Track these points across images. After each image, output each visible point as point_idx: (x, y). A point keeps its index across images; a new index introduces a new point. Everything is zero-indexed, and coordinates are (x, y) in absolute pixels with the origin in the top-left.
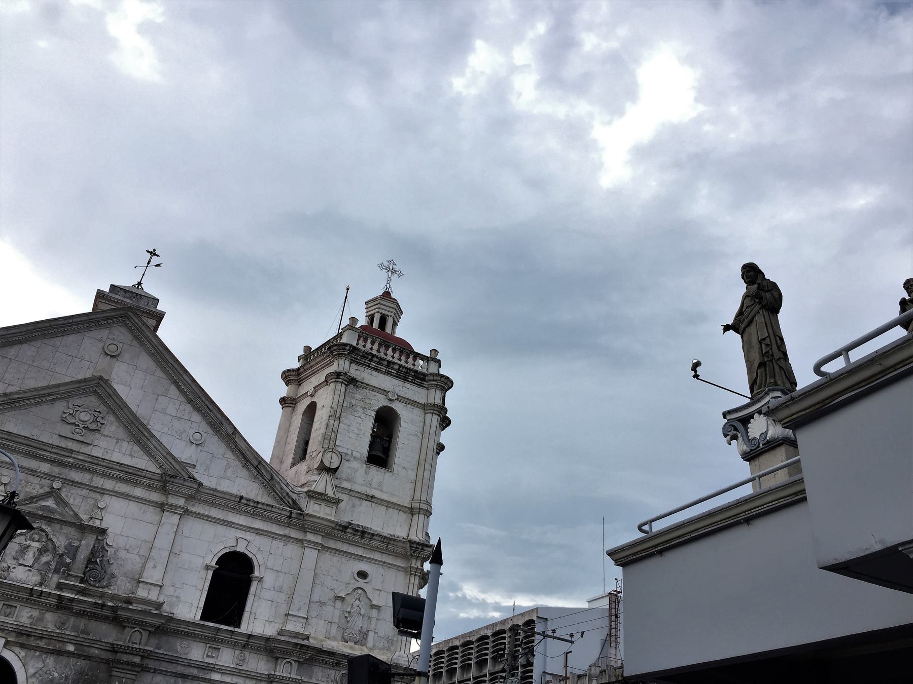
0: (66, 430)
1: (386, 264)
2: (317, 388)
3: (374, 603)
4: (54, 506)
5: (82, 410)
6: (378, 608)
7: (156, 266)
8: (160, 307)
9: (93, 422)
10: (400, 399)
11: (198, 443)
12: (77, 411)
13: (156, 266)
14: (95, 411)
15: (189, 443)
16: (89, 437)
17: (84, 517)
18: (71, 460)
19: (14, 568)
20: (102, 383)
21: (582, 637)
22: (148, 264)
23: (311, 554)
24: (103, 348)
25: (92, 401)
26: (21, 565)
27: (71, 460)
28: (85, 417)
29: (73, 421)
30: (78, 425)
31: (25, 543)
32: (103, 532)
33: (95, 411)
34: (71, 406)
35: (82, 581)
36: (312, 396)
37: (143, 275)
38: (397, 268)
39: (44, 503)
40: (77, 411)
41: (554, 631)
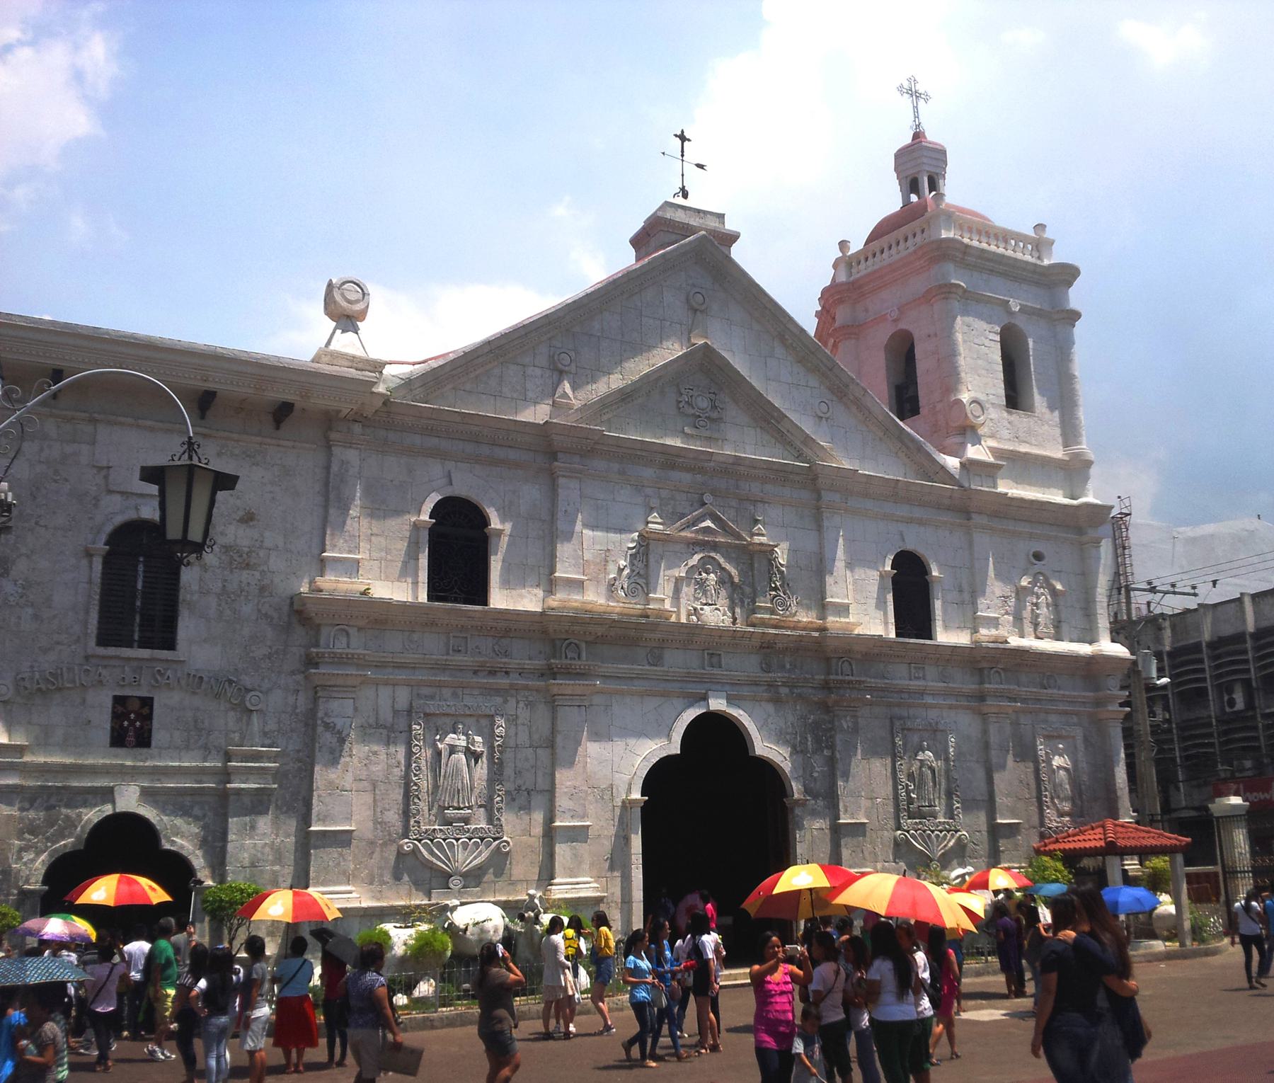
1: (906, 85)
2: (902, 309)
4: (712, 525)
8: (730, 225)
11: (827, 415)
12: (691, 396)
15: (817, 419)
18: (712, 464)
19: (702, 609)
21: (1214, 587)
22: (682, 156)
24: (688, 300)
26: (706, 604)
27: (712, 464)
29: (691, 411)
30: (700, 417)
34: (683, 391)
37: (683, 175)
38: (921, 88)
39: (703, 525)
40: (691, 396)
41: (1173, 586)
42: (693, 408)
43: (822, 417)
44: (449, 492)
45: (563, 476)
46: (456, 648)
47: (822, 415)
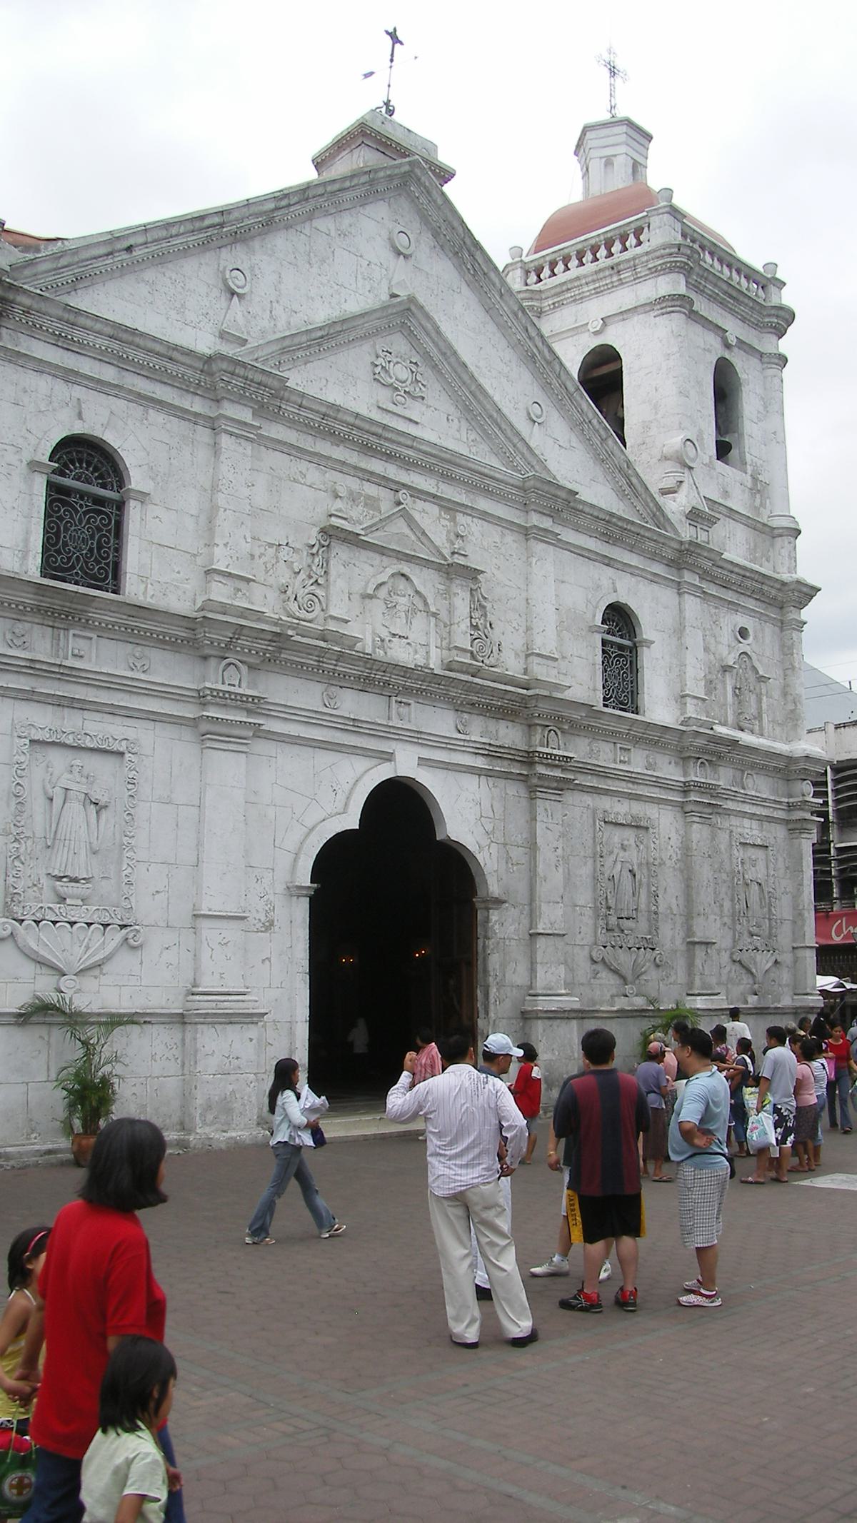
0: (384, 396)
3: (761, 673)
5: (395, 361)
6: (762, 679)
7: (372, 73)
9: (412, 382)
10: (741, 343)
12: (389, 362)
13: (372, 73)
14: (411, 362)
16: (414, 411)
17: (446, 552)
18: (410, 452)
20: (413, 308)
23: (692, 605)
24: (390, 240)
25: (399, 344)
28: (401, 372)
30: (397, 389)
31: (391, 599)
32: (472, 574)
33: (411, 362)
35: (473, 657)
36: (597, 333)
40: (389, 362)
42: (391, 377)
43: (535, 422)
44: (78, 428)
45: (232, 434)
46: (76, 652)
47: (535, 419)
